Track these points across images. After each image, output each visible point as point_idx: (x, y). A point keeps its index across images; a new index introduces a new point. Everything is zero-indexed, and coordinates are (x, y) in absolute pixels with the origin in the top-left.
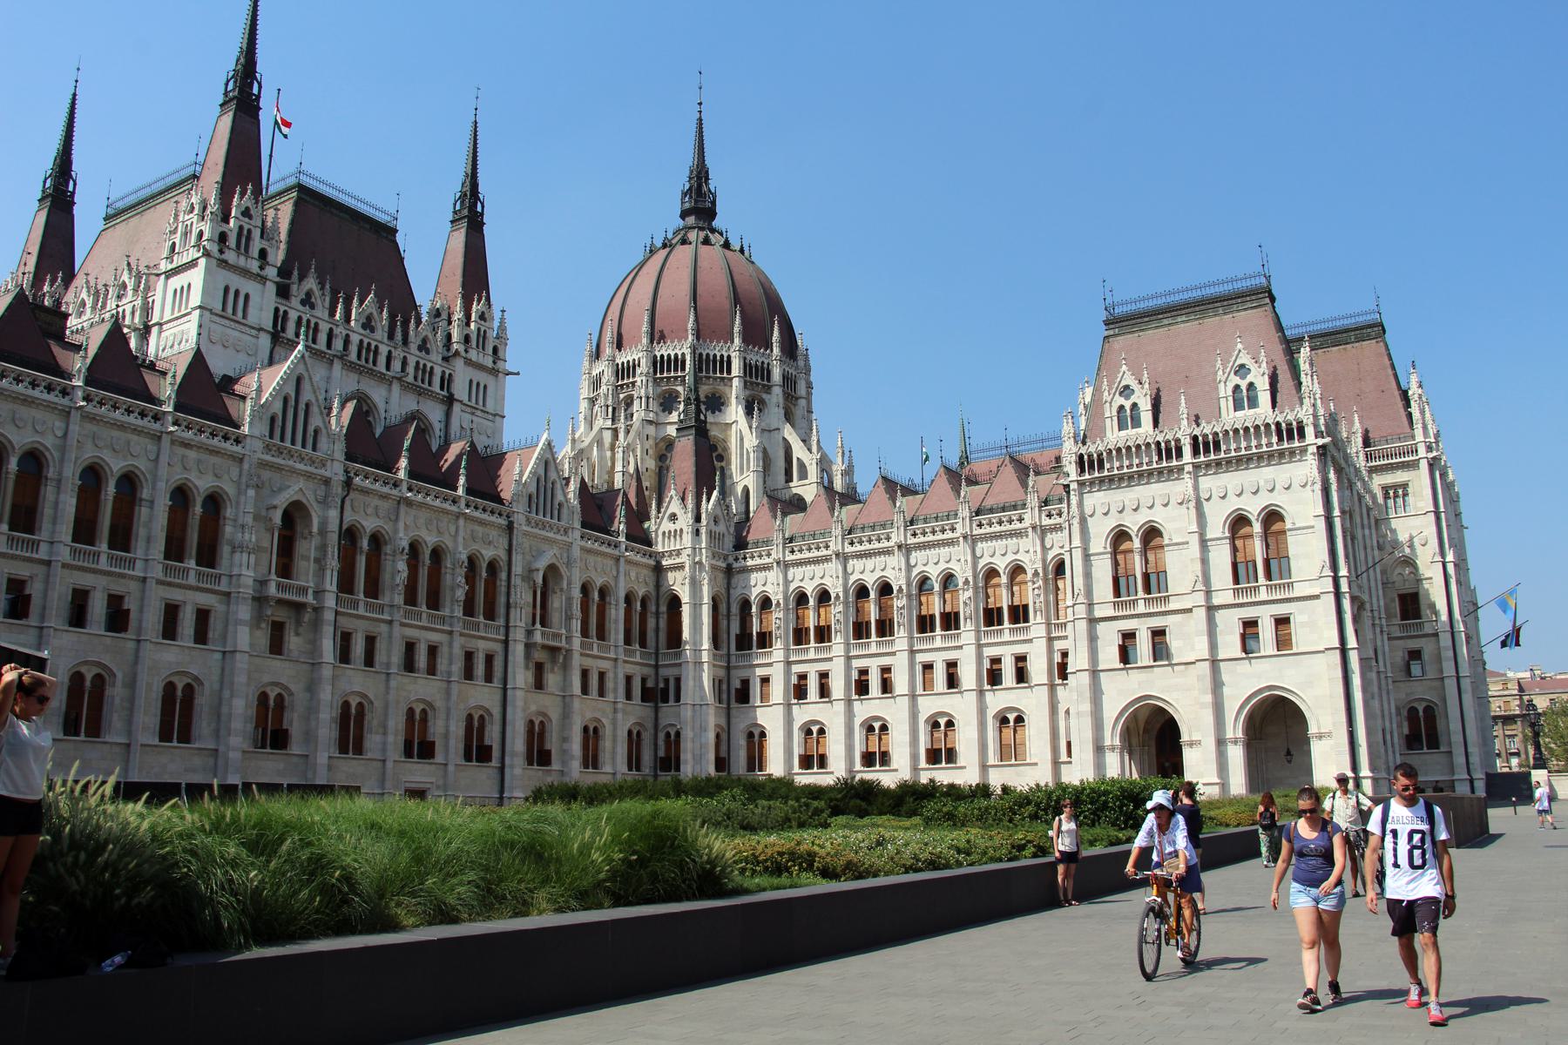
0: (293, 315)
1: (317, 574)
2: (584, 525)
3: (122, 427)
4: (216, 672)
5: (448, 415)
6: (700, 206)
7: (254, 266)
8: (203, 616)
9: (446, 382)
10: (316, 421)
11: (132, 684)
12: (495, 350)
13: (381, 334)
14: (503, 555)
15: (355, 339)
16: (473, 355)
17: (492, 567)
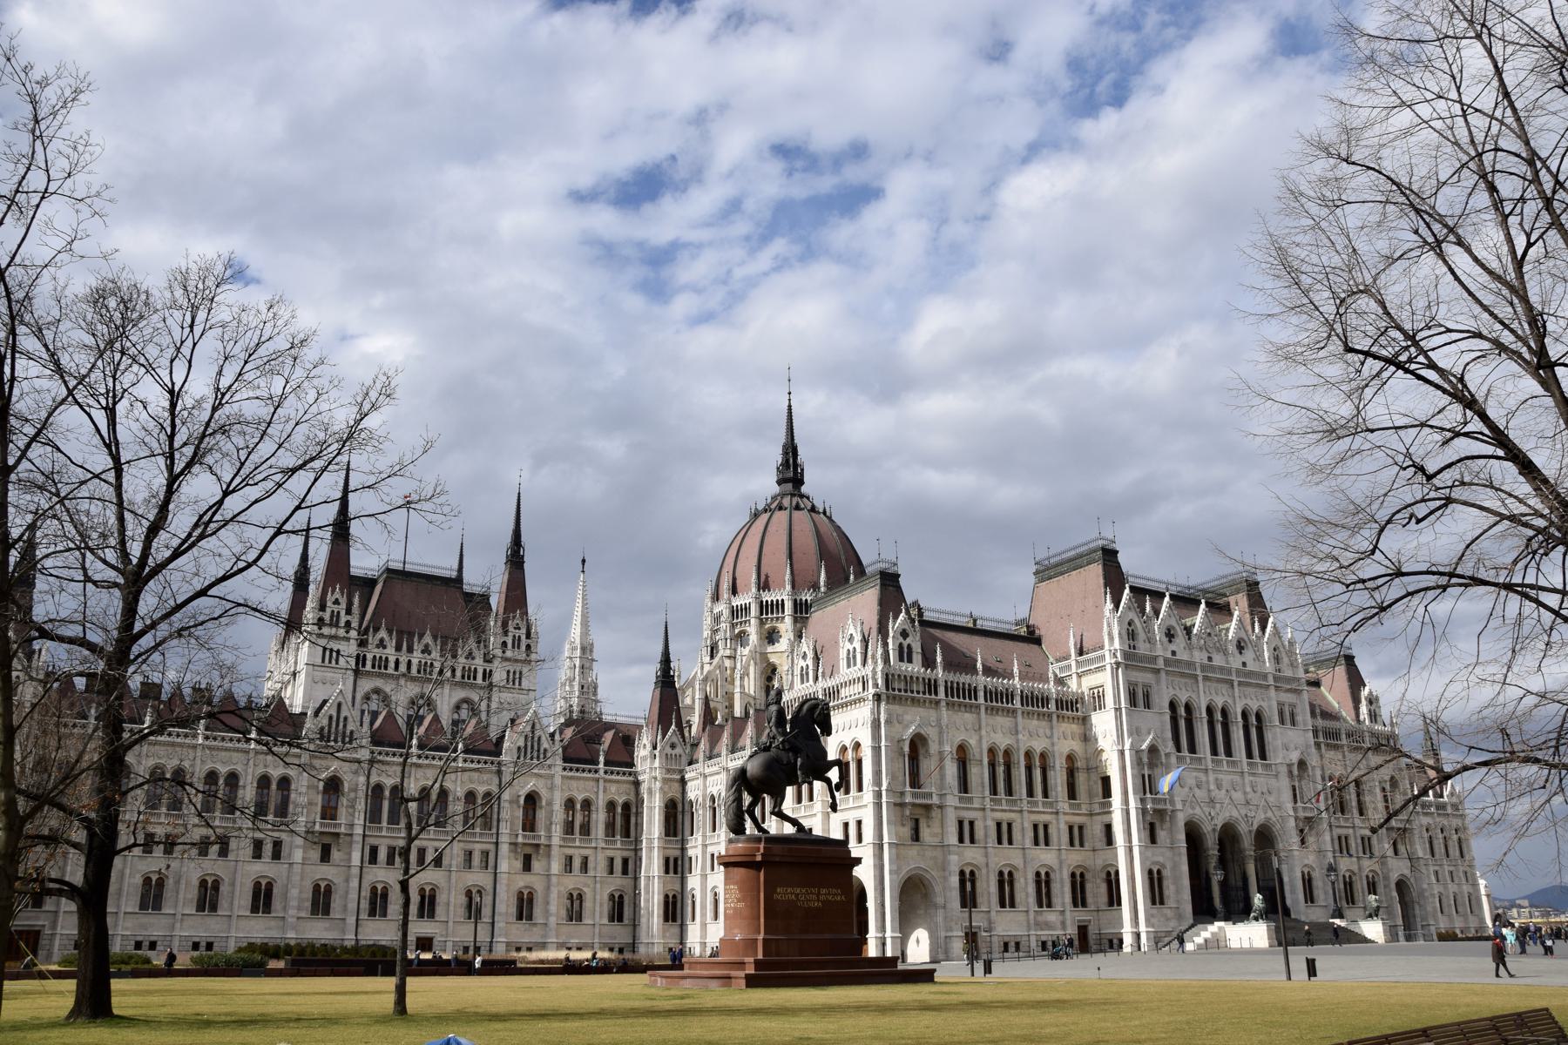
0: (369, 657)
1: (352, 816)
2: (565, 760)
3: (227, 749)
4: (285, 874)
6: (791, 473)
7: (341, 632)
8: (277, 845)
9: (487, 675)
10: (350, 727)
11: (233, 884)
12: (528, 647)
13: (435, 654)
14: (495, 789)
15: (415, 662)
16: (509, 654)
17: (488, 794)
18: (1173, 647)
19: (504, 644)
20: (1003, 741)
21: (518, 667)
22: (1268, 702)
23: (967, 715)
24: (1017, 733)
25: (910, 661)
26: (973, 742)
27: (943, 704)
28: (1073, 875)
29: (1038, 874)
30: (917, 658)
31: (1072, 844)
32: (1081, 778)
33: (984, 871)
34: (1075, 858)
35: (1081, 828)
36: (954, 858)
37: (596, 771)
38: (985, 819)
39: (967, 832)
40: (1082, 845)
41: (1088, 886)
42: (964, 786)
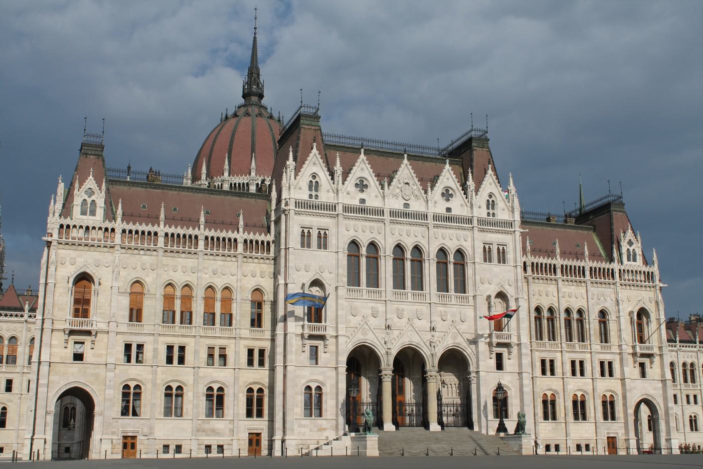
18: (363, 196)
20: (180, 279)
22: (471, 242)
25: (93, 213)
30: (100, 212)
33: (149, 386)
37: (22, 316)
39: (132, 353)
42: (136, 314)
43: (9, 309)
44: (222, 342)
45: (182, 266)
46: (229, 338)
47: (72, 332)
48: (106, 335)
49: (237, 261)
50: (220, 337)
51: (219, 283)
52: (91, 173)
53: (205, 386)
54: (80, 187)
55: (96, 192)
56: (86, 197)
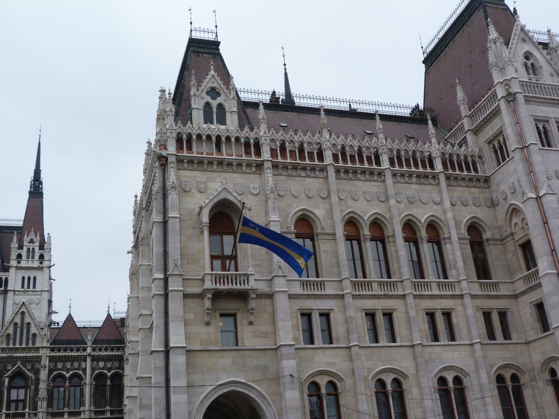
5: (5, 300)
12: (42, 257)
16: (23, 264)
19: (19, 256)
21: (32, 274)
23: (308, 180)
24: (387, 199)
25: (222, 121)
26: (319, 212)
27: (268, 165)
28: (500, 379)
29: (442, 381)
31: (491, 335)
32: (493, 253)
33: (348, 382)
34: (500, 355)
35: (503, 315)
36: (289, 365)
38: (344, 309)
40: (507, 335)
41: (527, 393)
43: (69, 342)
44: (446, 304)
45: (364, 192)
46: (453, 297)
47: (217, 295)
48: (268, 301)
49: (438, 184)
50: (441, 297)
51: (422, 216)
52: (212, 68)
53: (436, 375)
54: (199, 85)
55: (222, 93)
56: (208, 99)
